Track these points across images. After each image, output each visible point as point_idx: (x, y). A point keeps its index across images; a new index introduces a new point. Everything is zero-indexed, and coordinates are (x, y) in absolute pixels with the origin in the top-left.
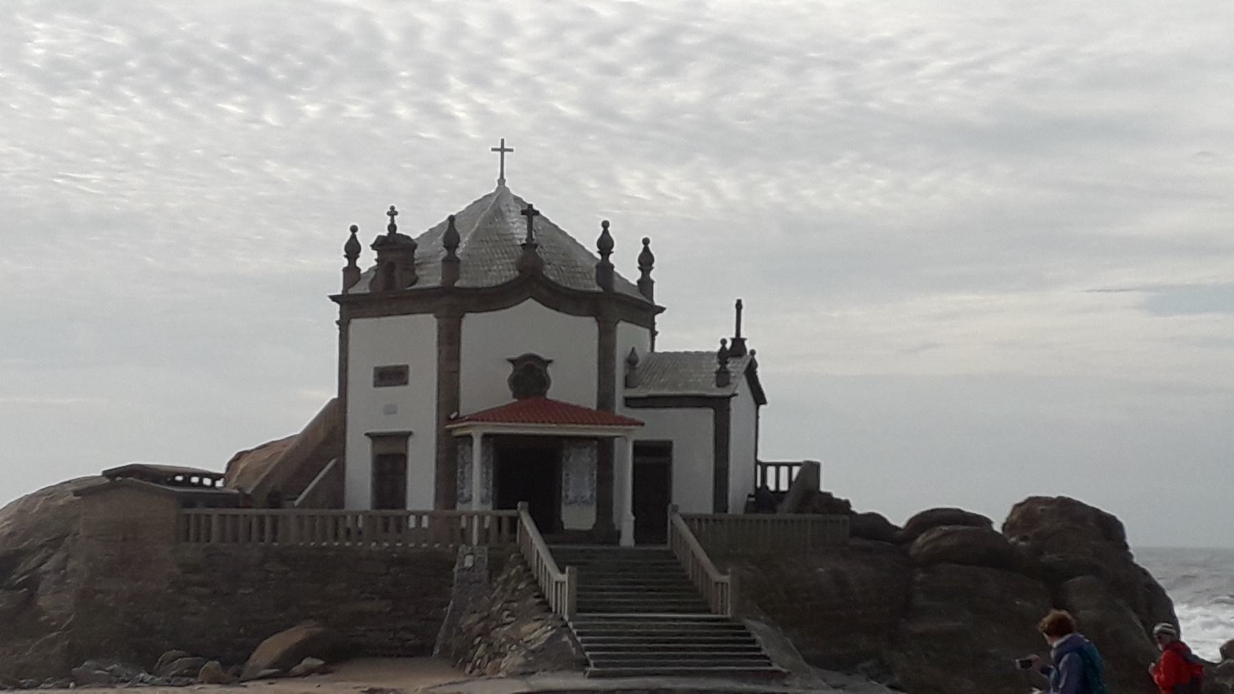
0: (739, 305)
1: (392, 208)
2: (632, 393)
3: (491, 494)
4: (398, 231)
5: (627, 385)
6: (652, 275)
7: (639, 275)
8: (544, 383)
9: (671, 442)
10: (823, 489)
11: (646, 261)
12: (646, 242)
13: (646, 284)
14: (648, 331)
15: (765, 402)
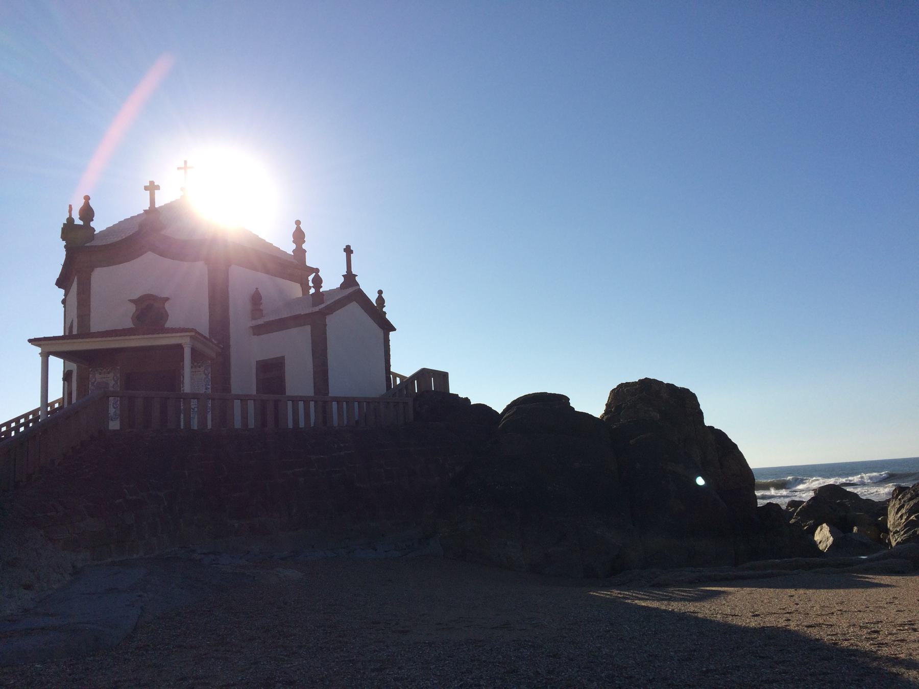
0: (348, 251)
1: (70, 206)
2: (255, 323)
3: (118, 412)
4: (75, 223)
5: (254, 318)
6: (304, 246)
7: (294, 246)
8: (164, 316)
9: (283, 358)
10: (450, 392)
11: (299, 236)
12: (298, 223)
13: (300, 253)
14: (299, 284)
15: (394, 329)
